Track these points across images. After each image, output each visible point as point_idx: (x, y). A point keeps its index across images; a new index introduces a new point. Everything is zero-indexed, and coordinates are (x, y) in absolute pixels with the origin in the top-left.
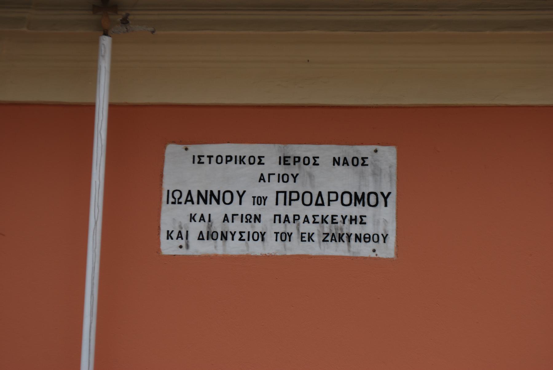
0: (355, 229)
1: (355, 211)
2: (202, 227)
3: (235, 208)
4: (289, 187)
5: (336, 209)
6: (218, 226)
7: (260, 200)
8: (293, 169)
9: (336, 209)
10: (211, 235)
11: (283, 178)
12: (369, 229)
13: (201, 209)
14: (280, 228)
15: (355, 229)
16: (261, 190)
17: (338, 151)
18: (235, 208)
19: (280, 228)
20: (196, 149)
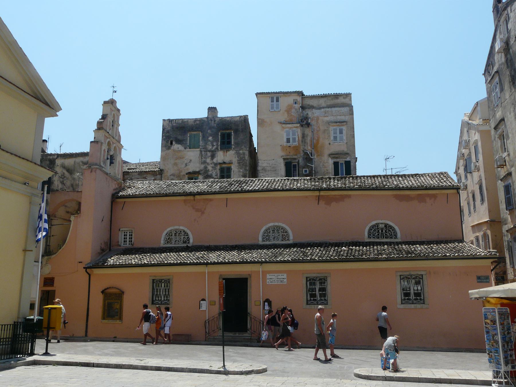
0: (283, 281)
1: (283, 280)
2: (270, 281)
3: (273, 280)
4: (277, 278)
5: (281, 280)
6: (272, 281)
7: (275, 279)
8: (278, 276)
9: (281, 280)
10: (271, 282)
11: (277, 277)
12: (284, 281)
13: (270, 280)
14: (277, 281)
15: (283, 281)
16: (275, 278)
17: (281, 274)
18: (273, 280)
19: (277, 281)
20: (270, 274)
